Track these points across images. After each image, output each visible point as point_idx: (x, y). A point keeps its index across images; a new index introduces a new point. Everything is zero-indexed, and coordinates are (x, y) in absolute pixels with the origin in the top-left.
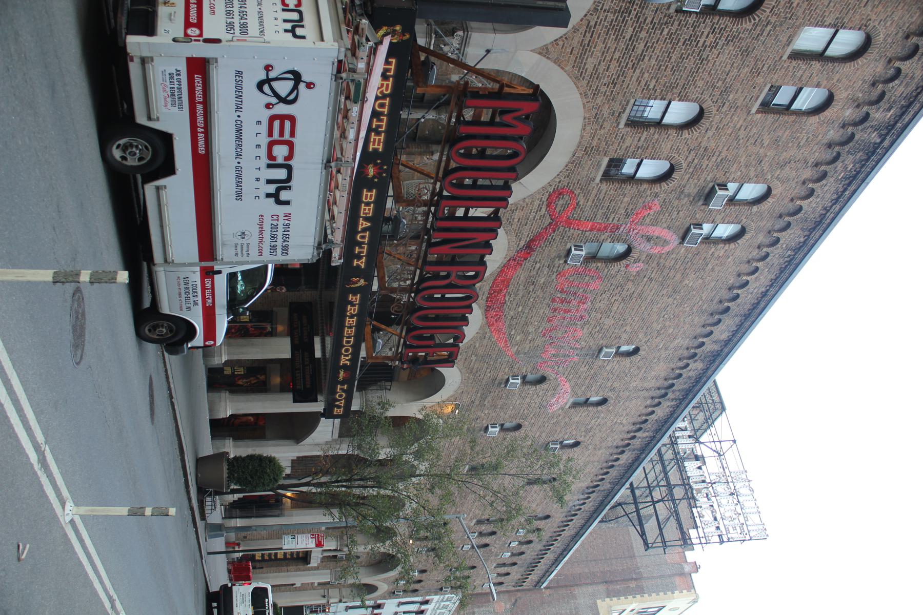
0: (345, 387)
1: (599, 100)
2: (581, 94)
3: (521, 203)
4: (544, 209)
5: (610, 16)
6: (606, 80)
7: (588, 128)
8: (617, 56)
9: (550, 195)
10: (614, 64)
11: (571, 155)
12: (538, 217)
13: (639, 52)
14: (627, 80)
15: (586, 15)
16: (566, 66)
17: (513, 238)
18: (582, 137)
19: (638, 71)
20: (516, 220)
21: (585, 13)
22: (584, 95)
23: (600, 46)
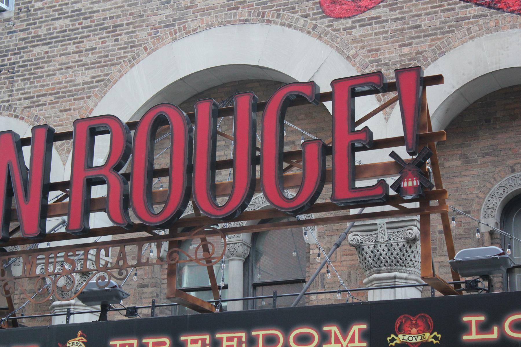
0: (473, 320)
1: (142, 34)
2: (132, 67)
3: (357, 60)
4: (373, 13)
5: (19, 84)
6: (110, 43)
7: (193, 25)
8: (72, 48)
9: (338, 18)
10: (87, 44)
11: (246, 26)
12: (397, 14)
13: (68, 21)
14: (108, 14)
15: (16, 117)
16: (88, 108)
17: (458, 34)
18: (210, 26)
19: (96, 7)
20: (406, 50)
21: (13, 120)
22: (134, 60)
23: (59, 77)
